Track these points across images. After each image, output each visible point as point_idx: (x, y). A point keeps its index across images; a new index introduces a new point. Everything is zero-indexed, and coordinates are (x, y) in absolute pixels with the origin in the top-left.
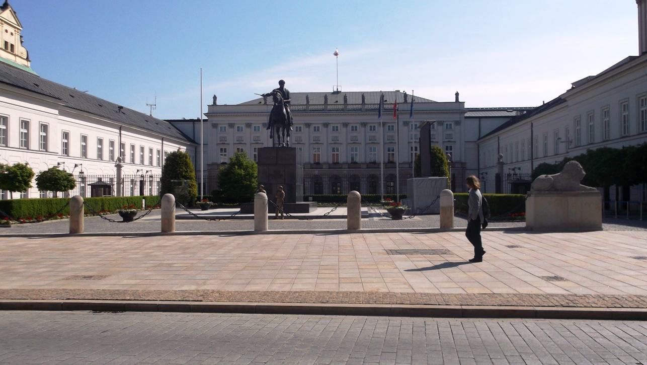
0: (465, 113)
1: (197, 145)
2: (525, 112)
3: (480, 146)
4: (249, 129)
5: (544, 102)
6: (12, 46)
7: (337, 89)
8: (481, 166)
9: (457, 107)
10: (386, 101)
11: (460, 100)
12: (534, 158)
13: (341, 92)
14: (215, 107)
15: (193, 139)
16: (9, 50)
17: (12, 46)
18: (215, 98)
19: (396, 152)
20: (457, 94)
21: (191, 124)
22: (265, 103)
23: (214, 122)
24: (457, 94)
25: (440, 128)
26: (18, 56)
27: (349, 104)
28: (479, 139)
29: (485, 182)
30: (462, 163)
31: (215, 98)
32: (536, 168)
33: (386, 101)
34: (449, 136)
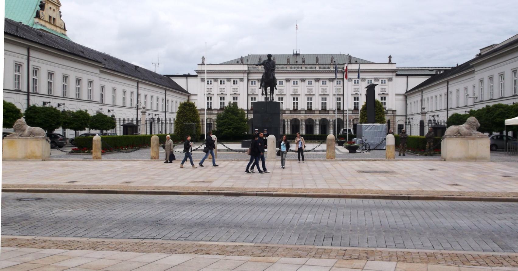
0: (396, 71)
1: (189, 95)
2: (442, 72)
3: (407, 97)
5: (457, 64)
7: (297, 52)
8: (408, 113)
10: (335, 62)
11: (392, 62)
12: (449, 108)
13: (299, 54)
14: (203, 66)
15: (186, 90)
18: (203, 58)
19: (341, 102)
20: (390, 57)
22: (242, 62)
23: (202, 78)
24: (390, 57)
28: (407, 92)
29: (411, 125)
30: (393, 111)
31: (203, 58)
32: (450, 117)
33: (335, 62)
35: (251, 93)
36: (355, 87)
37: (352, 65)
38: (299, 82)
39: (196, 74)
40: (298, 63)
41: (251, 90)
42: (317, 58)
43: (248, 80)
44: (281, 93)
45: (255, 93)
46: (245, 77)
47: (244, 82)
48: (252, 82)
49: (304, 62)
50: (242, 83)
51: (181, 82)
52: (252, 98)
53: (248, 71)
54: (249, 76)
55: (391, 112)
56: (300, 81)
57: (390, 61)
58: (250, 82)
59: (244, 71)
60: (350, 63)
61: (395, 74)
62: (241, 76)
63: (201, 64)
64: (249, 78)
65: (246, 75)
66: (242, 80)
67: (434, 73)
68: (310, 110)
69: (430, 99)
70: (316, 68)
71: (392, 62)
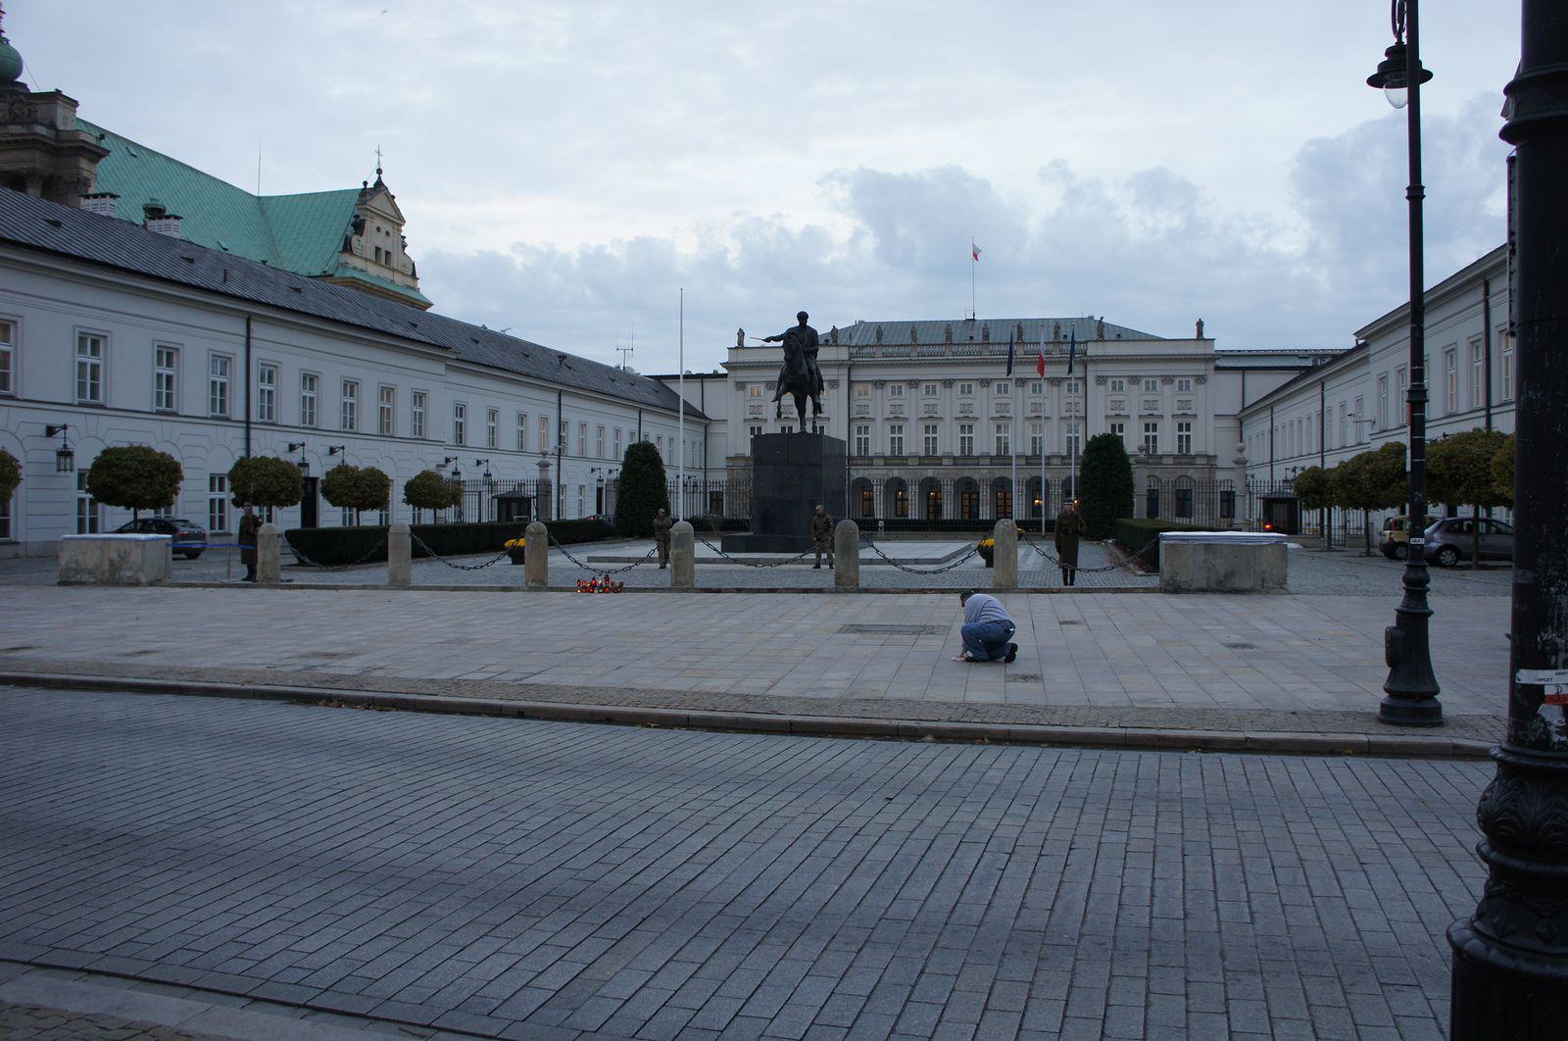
0: (1215, 359)
2: (1327, 360)
3: (1244, 424)
6: (388, 253)
9: (1199, 349)
10: (1065, 336)
11: (1205, 336)
16: (383, 263)
17: (388, 253)
18: (741, 334)
20: (1200, 324)
21: (696, 385)
22: (835, 341)
24: (1200, 324)
25: (1167, 389)
26: (397, 270)
27: (992, 344)
28: (1244, 409)
30: (1209, 457)
31: (741, 334)
33: (1065, 336)
34: (1184, 404)
35: (858, 416)
36: (1113, 398)
37: (1106, 344)
38: (975, 387)
39: (725, 371)
40: (974, 342)
41: (858, 408)
42: (1019, 327)
43: (850, 383)
44: (931, 415)
45: (867, 416)
47: (840, 388)
49: (986, 337)
50: (834, 392)
51: (687, 393)
52: (859, 429)
53: (849, 363)
54: (852, 373)
55: (1204, 461)
56: (979, 386)
57: (1200, 332)
58: (857, 388)
59: (838, 363)
60: (1101, 338)
61: (1211, 366)
63: (736, 348)
64: (852, 379)
65: (845, 371)
67: (1309, 363)
68: (1002, 458)
69: (1295, 424)
71: (1205, 336)
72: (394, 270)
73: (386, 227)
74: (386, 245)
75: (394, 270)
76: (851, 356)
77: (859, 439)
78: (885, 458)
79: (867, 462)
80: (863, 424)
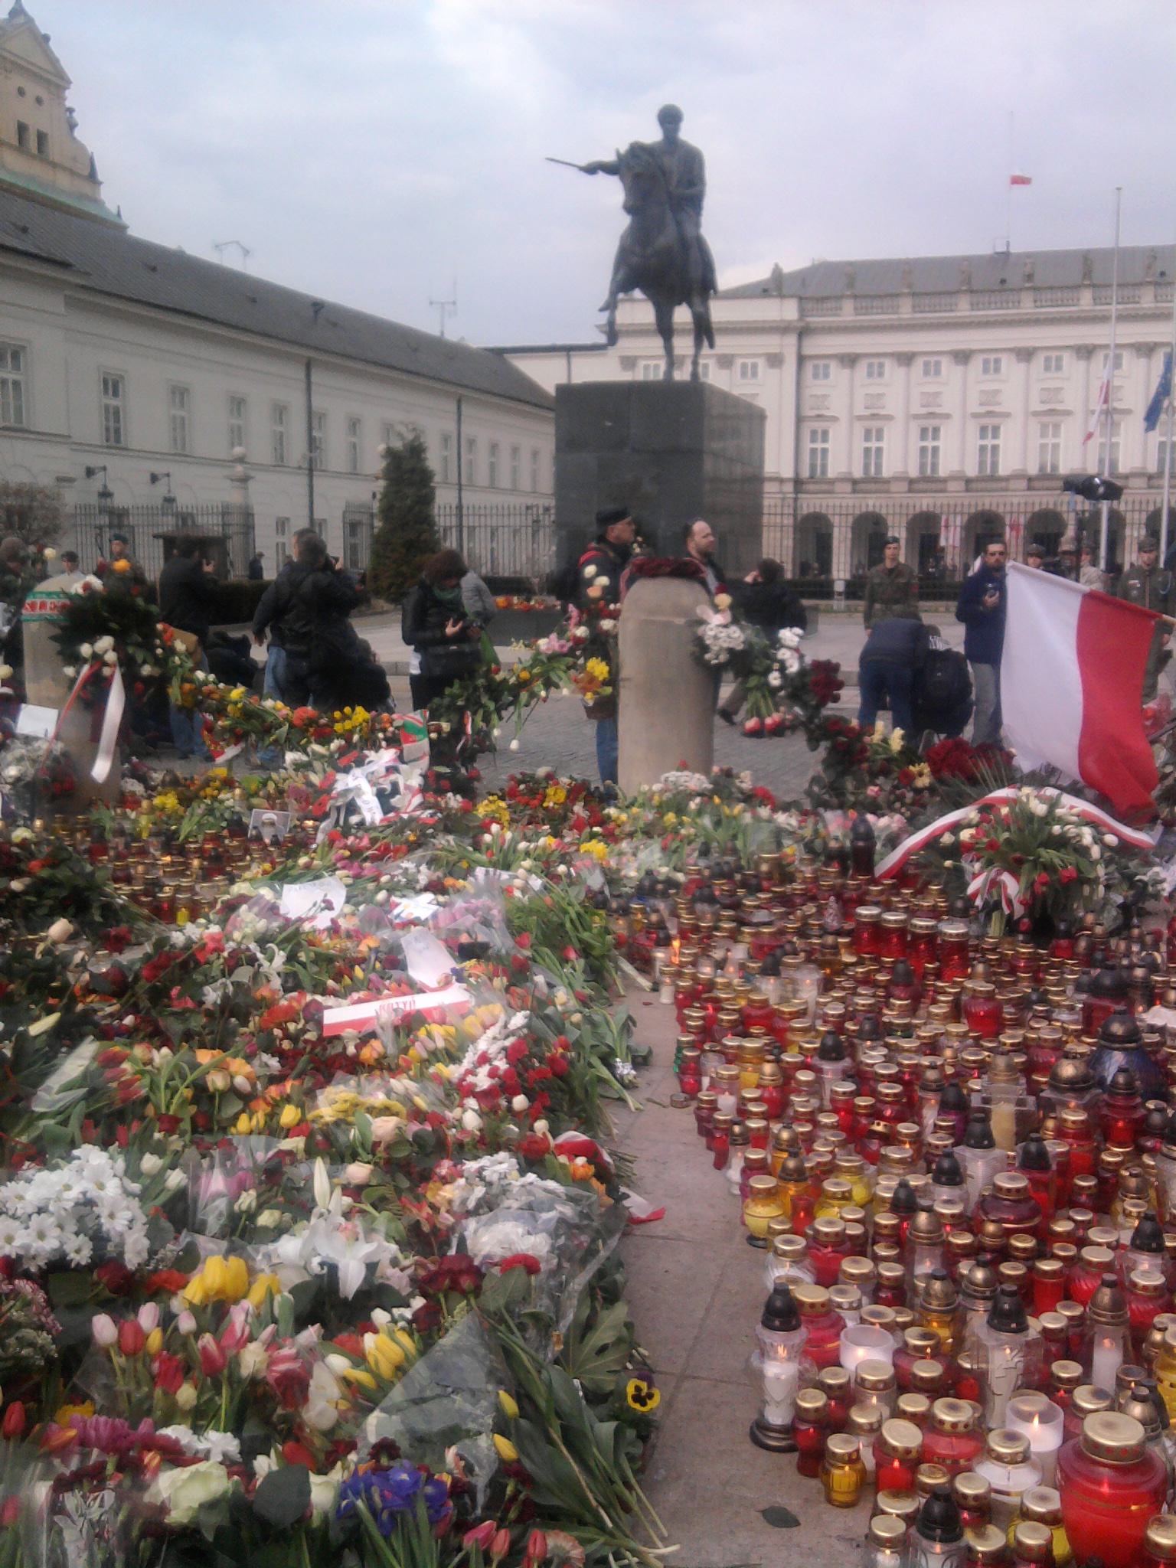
4: (727, 372)
6: (42, 138)
43: (801, 359)
46: (788, 346)
48: (816, 367)
49: (1030, 277)
52: (814, 433)
53: (802, 324)
56: (1013, 357)
62: (771, 343)
65: (792, 340)
66: (775, 360)
70: (1082, 302)
72: (54, 165)
73: (33, 90)
74: (36, 121)
75: (54, 165)
76: (802, 313)
77: (813, 451)
78: (855, 482)
79: (824, 487)
80: (819, 426)
